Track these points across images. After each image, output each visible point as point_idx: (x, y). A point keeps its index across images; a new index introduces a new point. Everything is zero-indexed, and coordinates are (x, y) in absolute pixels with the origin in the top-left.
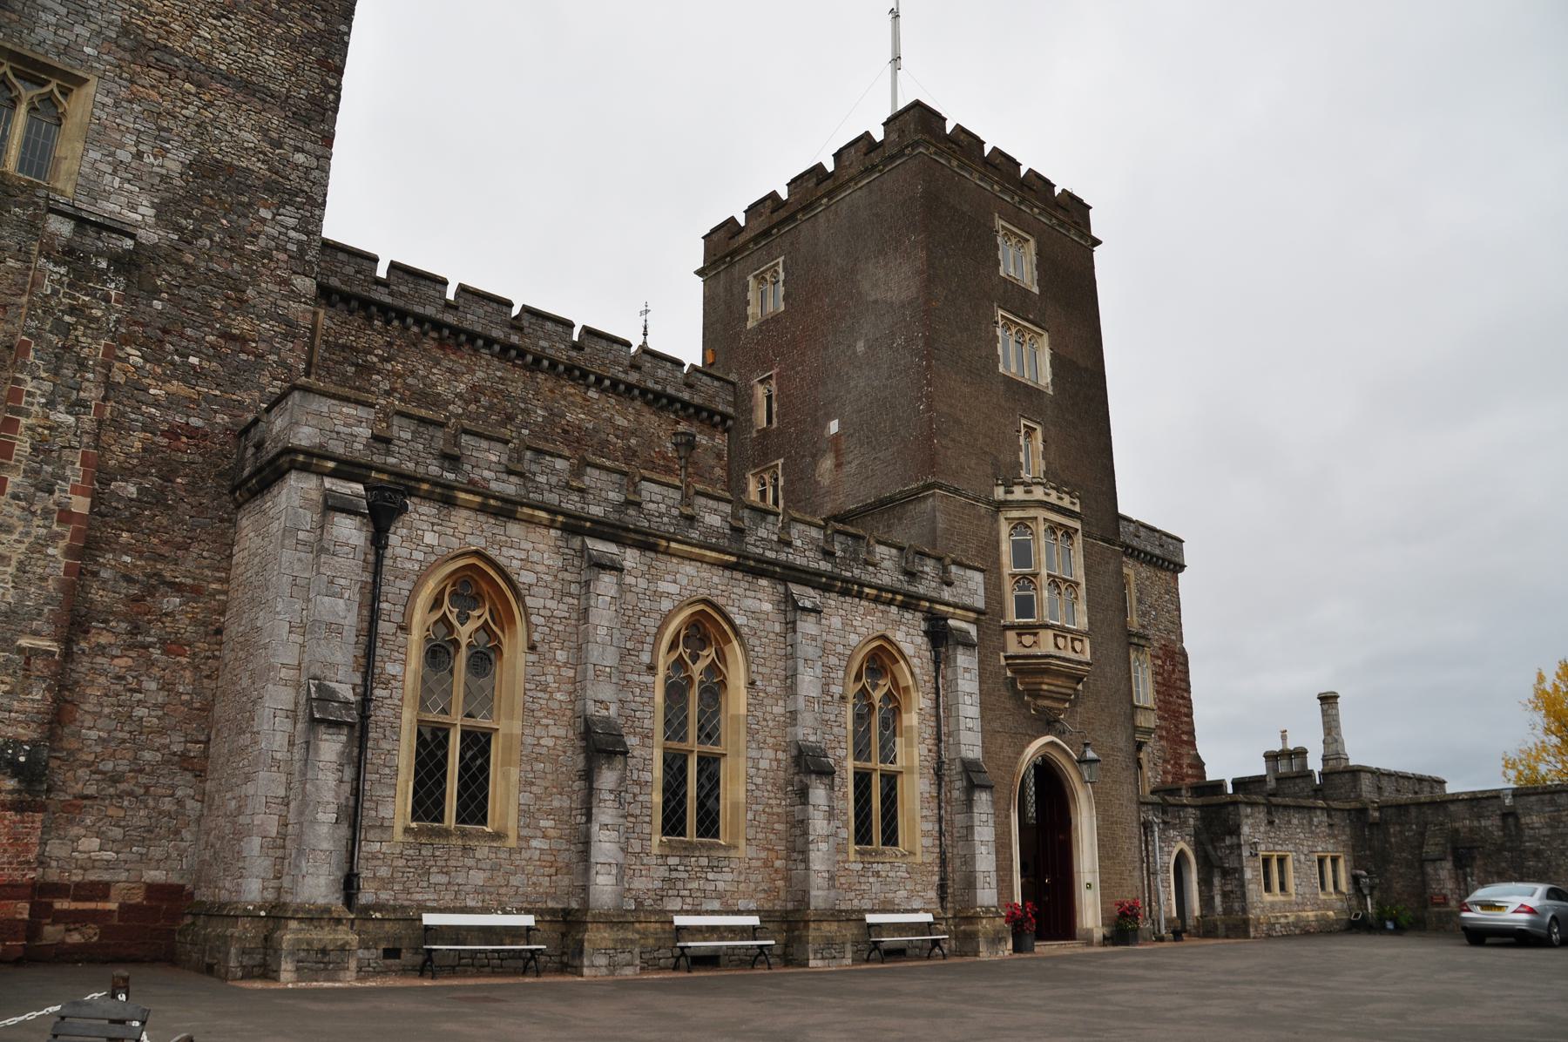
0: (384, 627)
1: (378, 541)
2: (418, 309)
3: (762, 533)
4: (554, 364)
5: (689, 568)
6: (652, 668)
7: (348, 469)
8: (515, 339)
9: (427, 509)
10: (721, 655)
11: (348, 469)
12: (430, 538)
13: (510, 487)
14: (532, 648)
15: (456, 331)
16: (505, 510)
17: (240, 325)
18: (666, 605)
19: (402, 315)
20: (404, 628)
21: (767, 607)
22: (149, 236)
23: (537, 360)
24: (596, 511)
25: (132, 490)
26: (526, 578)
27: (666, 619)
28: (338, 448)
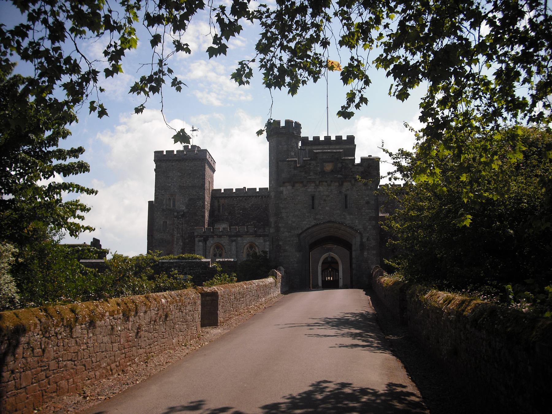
0: (207, 253)
1: (206, 244)
2: (240, 195)
3: (260, 231)
4: (265, 197)
5: (248, 238)
6: (243, 253)
7: (201, 236)
8: (257, 195)
9: (211, 239)
10: (255, 249)
11: (201, 236)
12: (212, 242)
13: (221, 234)
14: (226, 252)
15: (247, 197)
16: (220, 237)
17: (197, 218)
18: (245, 244)
19: (238, 197)
20: (209, 253)
21: (262, 241)
22: (185, 211)
23: (262, 197)
24: (233, 234)
25: (188, 241)
26: (224, 244)
27: (245, 246)
28: (199, 234)
